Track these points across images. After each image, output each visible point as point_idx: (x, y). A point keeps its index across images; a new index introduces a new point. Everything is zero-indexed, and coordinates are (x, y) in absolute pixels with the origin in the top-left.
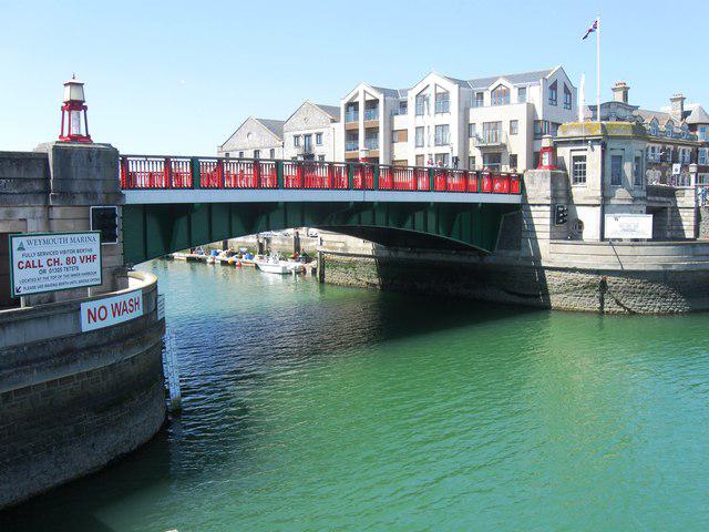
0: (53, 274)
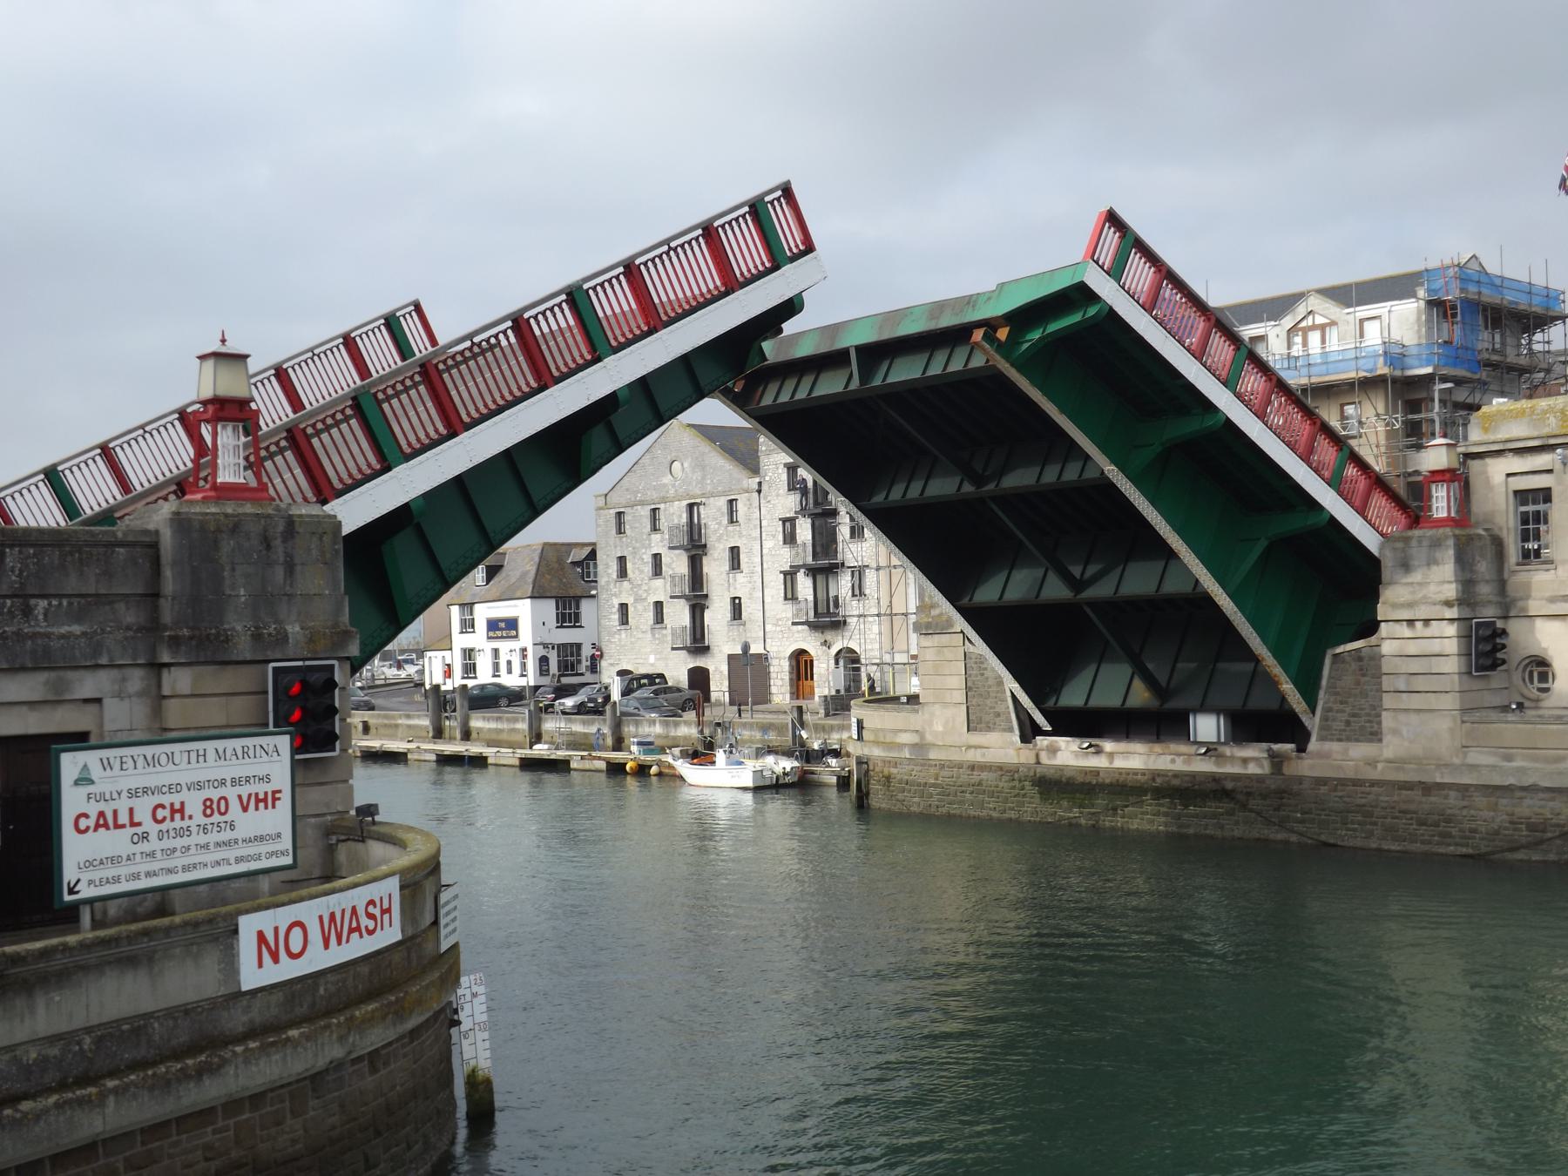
0: (168, 843)
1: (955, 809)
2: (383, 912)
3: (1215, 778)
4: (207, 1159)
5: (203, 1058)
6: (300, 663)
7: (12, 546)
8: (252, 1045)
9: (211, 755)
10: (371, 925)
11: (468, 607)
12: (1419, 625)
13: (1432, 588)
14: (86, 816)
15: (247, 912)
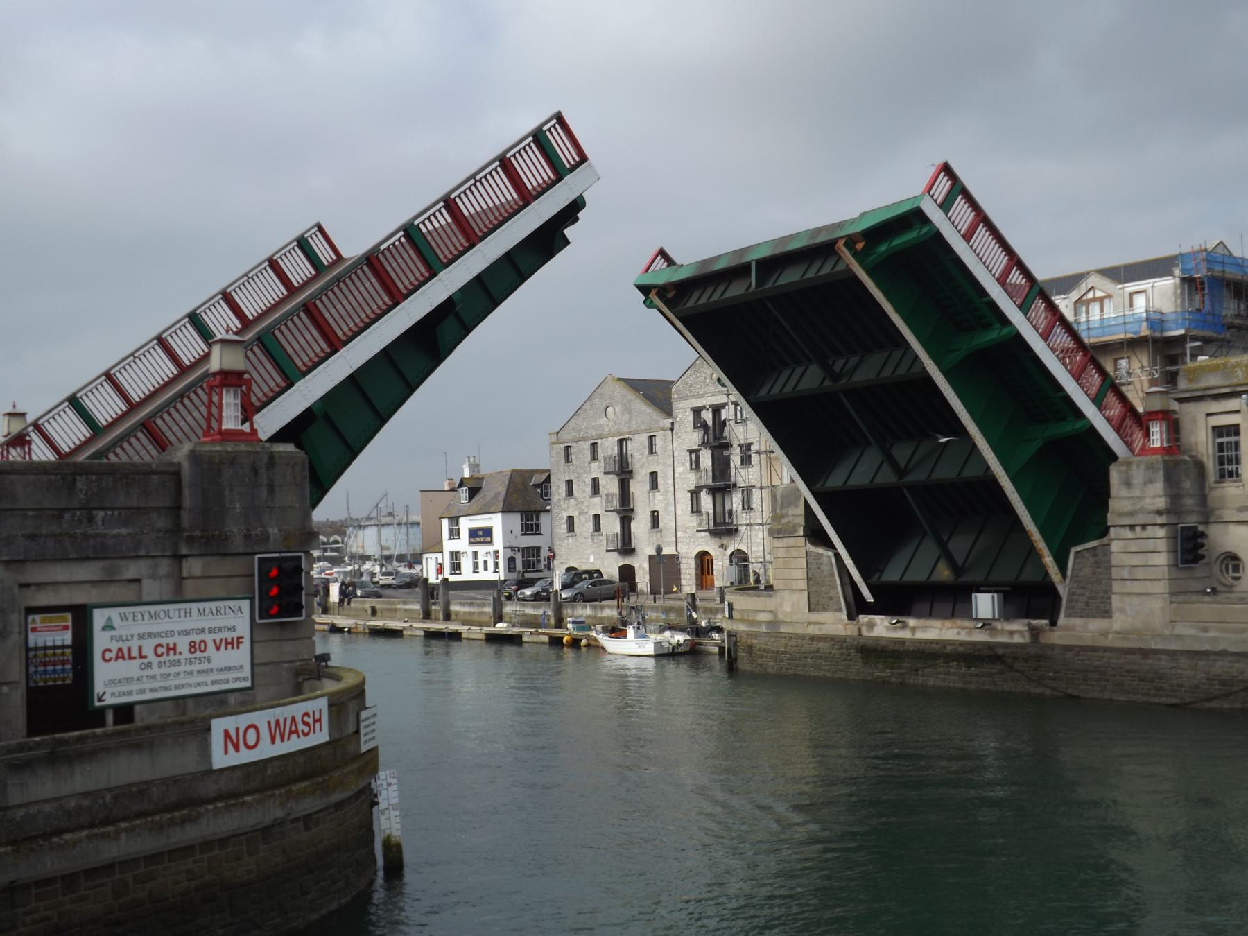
0: (165, 670)
1: (800, 670)
2: (315, 721)
3: (990, 646)
4: (189, 880)
5: (185, 812)
6: (277, 555)
7: (80, 475)
8: (219, 805)
9: (195, 612)
10: (306, 729)
11: (455, 519)
12: (1138, 529)
13: (1148, 501)
14: (110, 650)
15: (218, 716)
